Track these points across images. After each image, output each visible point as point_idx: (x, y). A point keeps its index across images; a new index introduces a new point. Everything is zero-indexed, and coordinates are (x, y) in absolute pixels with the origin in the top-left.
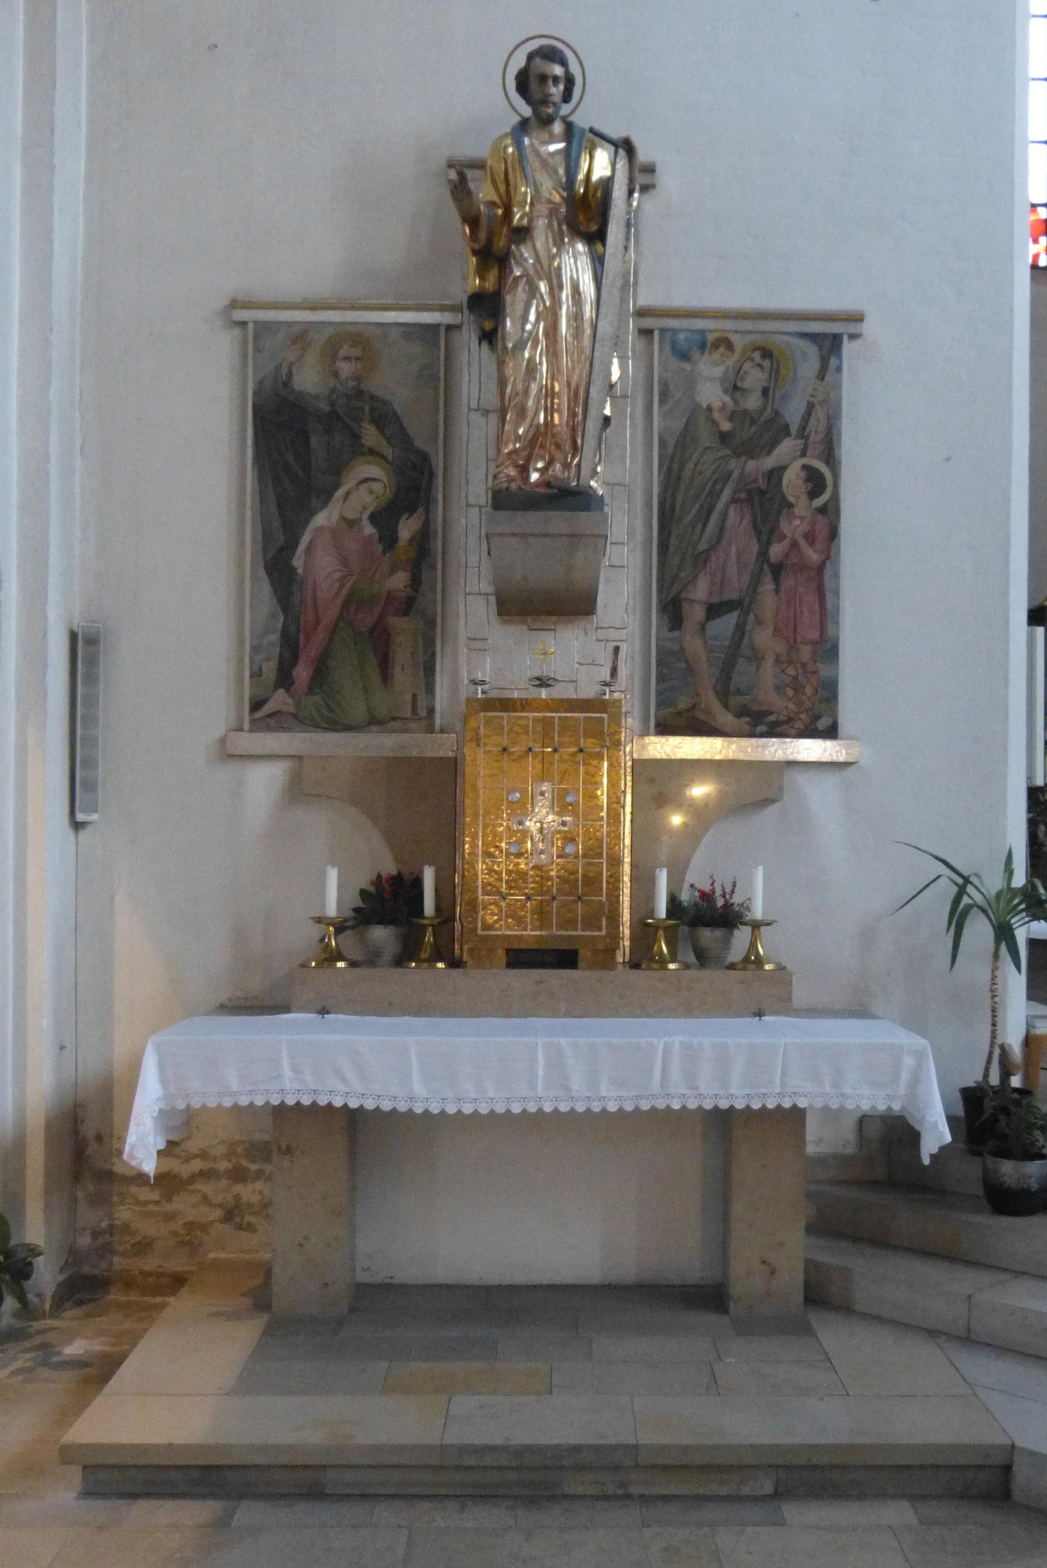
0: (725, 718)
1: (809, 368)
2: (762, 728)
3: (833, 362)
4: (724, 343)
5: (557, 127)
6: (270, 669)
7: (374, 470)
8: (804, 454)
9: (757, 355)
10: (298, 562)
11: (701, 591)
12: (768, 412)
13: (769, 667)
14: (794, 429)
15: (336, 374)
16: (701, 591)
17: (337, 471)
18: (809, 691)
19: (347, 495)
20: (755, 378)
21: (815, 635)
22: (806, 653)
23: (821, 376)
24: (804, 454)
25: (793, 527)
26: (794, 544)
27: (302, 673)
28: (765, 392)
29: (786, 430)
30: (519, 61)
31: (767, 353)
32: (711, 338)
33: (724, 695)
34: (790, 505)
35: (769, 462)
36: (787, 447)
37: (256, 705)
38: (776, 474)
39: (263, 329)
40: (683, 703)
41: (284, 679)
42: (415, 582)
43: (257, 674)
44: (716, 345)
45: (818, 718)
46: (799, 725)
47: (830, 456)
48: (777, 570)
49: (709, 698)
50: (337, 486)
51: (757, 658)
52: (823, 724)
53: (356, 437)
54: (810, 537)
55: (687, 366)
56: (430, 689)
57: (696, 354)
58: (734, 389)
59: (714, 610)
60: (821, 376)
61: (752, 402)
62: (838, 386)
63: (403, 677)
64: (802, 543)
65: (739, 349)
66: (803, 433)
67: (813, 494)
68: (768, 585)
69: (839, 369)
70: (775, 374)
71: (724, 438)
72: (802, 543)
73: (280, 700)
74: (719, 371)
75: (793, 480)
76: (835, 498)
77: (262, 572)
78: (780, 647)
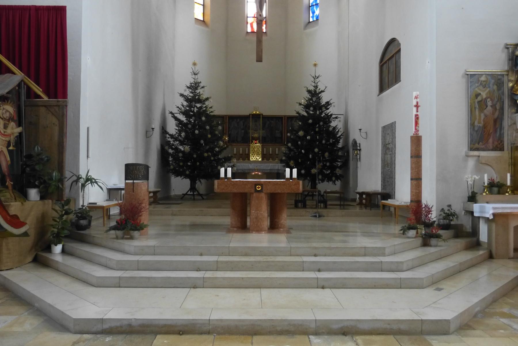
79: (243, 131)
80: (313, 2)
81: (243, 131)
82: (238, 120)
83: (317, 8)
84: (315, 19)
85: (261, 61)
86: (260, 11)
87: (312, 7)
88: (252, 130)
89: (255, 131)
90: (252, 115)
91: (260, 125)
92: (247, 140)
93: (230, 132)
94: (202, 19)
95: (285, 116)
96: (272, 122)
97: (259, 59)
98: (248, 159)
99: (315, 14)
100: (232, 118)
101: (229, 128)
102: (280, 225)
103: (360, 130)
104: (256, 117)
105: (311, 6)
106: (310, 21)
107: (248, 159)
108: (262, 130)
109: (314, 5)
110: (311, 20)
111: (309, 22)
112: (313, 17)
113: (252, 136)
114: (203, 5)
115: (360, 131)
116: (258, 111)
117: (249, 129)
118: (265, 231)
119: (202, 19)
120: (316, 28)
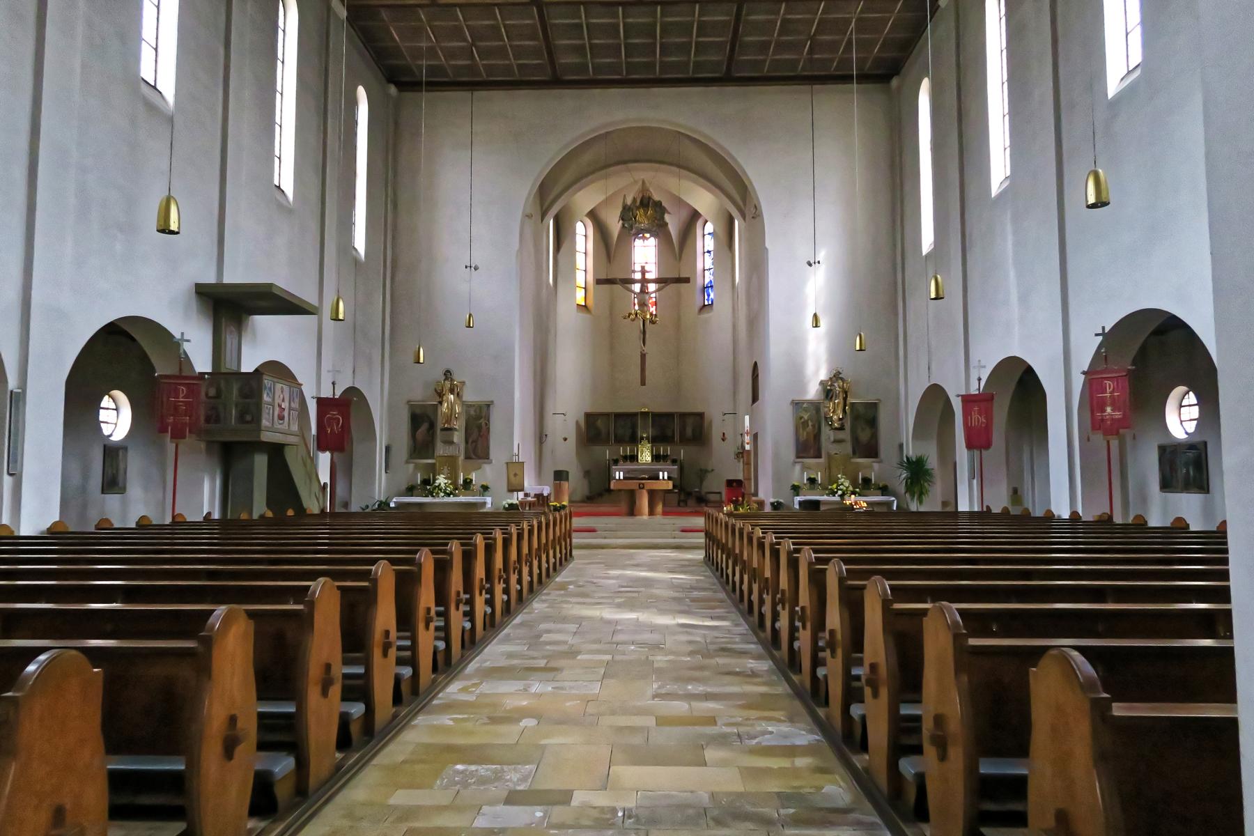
0: (474, 457)
1: (485, 409)
4: (474, 406)
16: (470, 441)
20: (478, 411)
35: (480, 422)
38: (481, 423)
41: (415, 451)
49: (472, 454)
76: (489, 428)
84: (710, 303)
92: (634, 440)
94: (584, 304)
95: (676, 413)
100: (618, 416)
104: (645, 414)
105: (707, 287)
110: (706, 303)
111: (704, 305)
112: (708, 300)
114: (585, 288)
119: (584, 304)
120: (711, 314)
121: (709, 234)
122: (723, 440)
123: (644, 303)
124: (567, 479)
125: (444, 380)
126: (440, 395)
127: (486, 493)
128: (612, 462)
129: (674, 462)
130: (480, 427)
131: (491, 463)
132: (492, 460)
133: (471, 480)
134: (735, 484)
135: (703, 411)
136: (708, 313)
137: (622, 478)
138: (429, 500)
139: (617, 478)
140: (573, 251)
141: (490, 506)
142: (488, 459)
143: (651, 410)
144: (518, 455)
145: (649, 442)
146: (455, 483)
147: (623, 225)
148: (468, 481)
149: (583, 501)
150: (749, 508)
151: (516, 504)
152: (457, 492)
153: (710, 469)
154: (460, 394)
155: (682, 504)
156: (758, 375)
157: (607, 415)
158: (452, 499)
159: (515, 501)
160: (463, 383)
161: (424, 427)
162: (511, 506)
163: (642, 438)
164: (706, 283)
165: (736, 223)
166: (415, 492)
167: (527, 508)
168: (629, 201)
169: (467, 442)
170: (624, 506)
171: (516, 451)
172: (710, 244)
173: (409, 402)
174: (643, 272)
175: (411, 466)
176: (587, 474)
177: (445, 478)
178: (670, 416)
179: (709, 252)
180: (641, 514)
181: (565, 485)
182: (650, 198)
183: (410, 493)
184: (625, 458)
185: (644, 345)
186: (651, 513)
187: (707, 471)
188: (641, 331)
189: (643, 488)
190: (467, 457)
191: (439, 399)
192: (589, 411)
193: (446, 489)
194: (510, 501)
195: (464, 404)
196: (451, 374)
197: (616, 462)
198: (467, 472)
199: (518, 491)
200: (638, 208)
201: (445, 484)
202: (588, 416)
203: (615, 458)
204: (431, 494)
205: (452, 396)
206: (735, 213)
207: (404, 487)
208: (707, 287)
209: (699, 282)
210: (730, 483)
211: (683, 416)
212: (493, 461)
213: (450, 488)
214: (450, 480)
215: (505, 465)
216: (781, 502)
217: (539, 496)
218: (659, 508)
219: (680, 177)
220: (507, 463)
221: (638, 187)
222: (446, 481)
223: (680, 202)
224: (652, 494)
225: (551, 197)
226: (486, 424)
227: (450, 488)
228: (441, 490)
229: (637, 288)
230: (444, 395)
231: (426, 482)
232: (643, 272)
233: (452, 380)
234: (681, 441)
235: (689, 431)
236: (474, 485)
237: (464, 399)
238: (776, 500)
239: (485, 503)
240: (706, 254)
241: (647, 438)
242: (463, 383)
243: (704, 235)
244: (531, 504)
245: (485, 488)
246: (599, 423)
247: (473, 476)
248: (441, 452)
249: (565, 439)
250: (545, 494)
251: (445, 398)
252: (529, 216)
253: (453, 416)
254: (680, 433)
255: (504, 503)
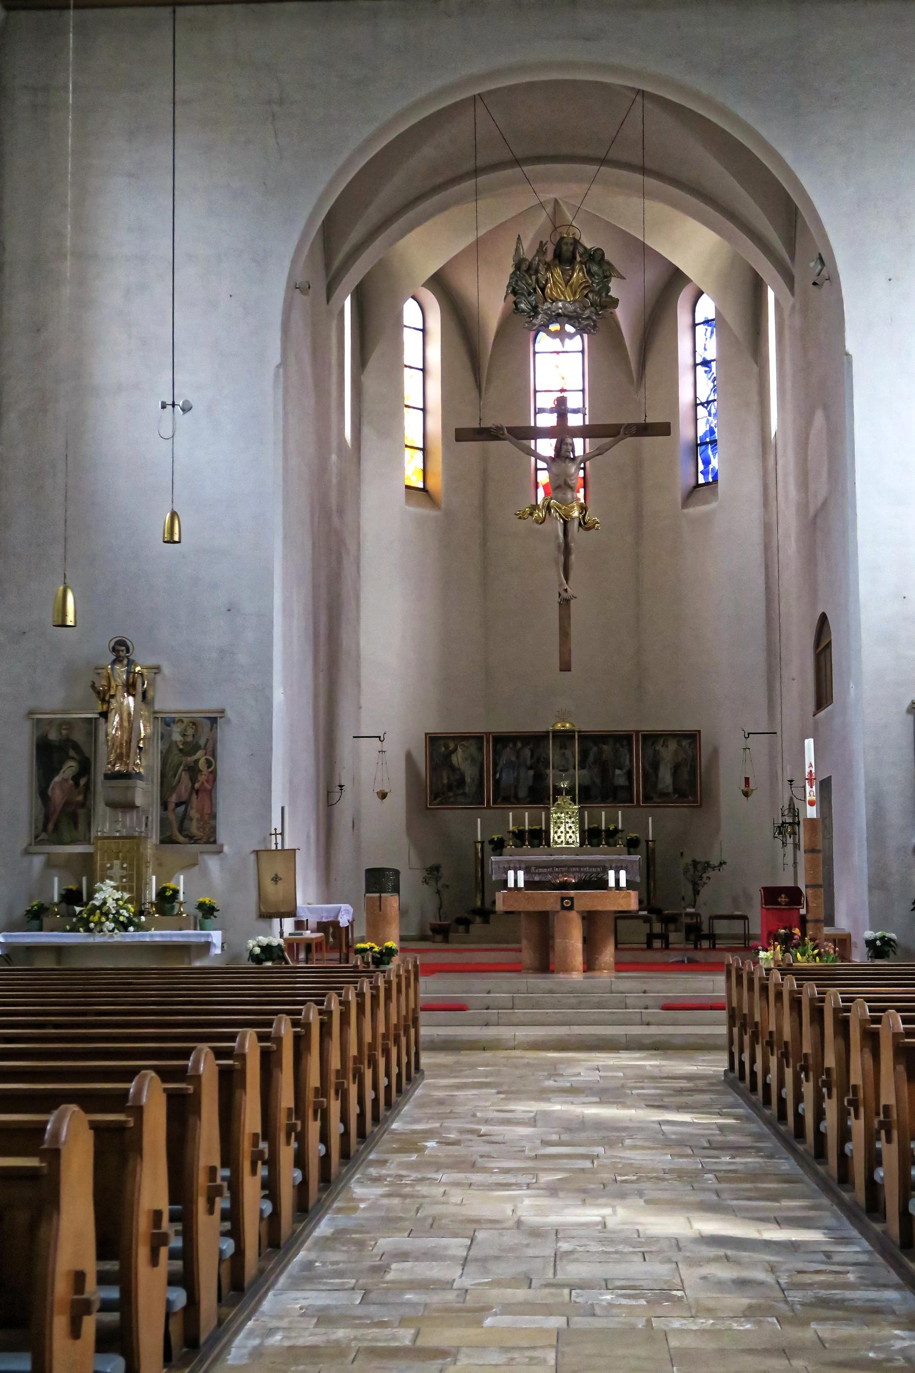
0: (181, 838)
1: (207, 728)
2: (192, 841)
3: (215, 725)
4: (181, 721)
5: (125, 662)
6: (40, 826)
7: (72, 763)
8: (206, 755)
9: (191, 724)
10: (50, 793)
11: (174, 799)
12: (194, 742)
13: (194, 822)
14: (203, 746)
15: (61, 734)
16: (174, 799)
17: (61, 763)
18: (207, 829)
19: (64, 772)
20: (190, 732)
21: (209, 812)
22: (206, 817)
23: (211, 730)
24: (206, 755)
25: (202, 778)
26: (203, 783)
27: (50, 827)
28: (194, 736)
29: (199, 748)
30: (112, 644)
31: (194, 724)
32: (177, 719)
33: (181, 830)
34: (201, 771)
36: (200, 754)
37: (36, 837)
38: (197, 761)
39: (39, 720)
40: (168, 834)
41: (45, 829)
42: (85, 798)
43: (36, 828)
44: (178, 721)
45: (210, 838)
46: (205, 840)
47: (214, 755)
48: (197, 792)
50: (61, 769)
51: (191, 819)
52: (212, 840)
53: (67, 753)
54: (207, 781)
55: (169, 728)
56: (90, 831)
57: (172, 724)
58: (184, 735)
59: (178, 805)
60: (211, 730)
61: (190, 739)
62: (216, 733)
63: (82, 827)
64: (205, 783)
65: (185, 722)
66: (205, 748)
67: (209, 767)
68: (194, 796)
69: (217, 728)
70: (196, 730)
71: (181, 750)
72: (205, 783)
73: (43, 836)
74: (179, 730)
75: (202, 764)
76: (215, 769)
77: (38, 796)
78: (198, 816)
79: (531, 773)
80: (705, 435)
81: (531, 773)
82: (519, 745)
83: (714, 450)
85: (570, 670)
86: (565, 582)
87: (703, 447)
88: (553, 768)
89: (561, 771)
90: (554, 732)
91: (574, 757)
93: (498, 775)
94: (421, 486)
96: (605, 747)
97: (565, 667)
98: (546, 845)
99: (711, 467)
100: (501, 740)
101: (495, 764)
102: (603, 965)
103: (791, 781)
104: (564, 738)
105: (702, 444)
106: (700, 482)
107: (546, 845)
108: (578, 770)
109: (706, 443)
110: (701, 480)
111: (698, 486)
112: (705, 473)
113: (555, 787)
114: (424, 450)
115: (791, 785)
116: (567, 722)
117: (547, 766)
118: (578, 971)
119: (421, 486)
120: (714, 505)
121: (707, 322)
122: (746, 794)
123: (566, 483)
124: (396, 889)
125: (114, 663)
126: (104, 697)
127: (208, 922)
128: (488, 848)
129: (632, 845)
130: (193, 770)
131: (220, 852)
132: (222, 846)
133: (176, 892)
134: (783, 899)
135: (695, 728)
136: (706, 502)
137: (521, 884)
138: (79, 937)
139: (511, 884)
140: (396, 366)
141: (218, 951)
142: (215, 842)
143: (576, 729)
144: (282, 834)
145: (573, 800)
146: (137, 899)
147: (516, 303)
148: (169, 893)
149: (423, 938)
150: (819, 954)
151: (279, 945)
152: (143, 918)
153: (715, 862)
154: (150, 694)
155: (657, 944)
156: (829, 645)
157: (478, 739)
158: (131, 936)
159: (276, 941)
160: (157, 669)
161: (70, 768)
162: (268, 950)
163: (558, 791)
164: (700, 434)
165: (771, 295)
166: (46, 921)
167: (302, 956)
168: (528, 250)
169: (164, 805)
170: (527, 956)
171: (276, 823)
172: (709, 347)
173: (31, 713)
174: (561, 408)
175: (38, 862)
176: (433, 872)
177: (116, 888)
178: (624, 739)
179: (706, 363)
180: (567, 969)
181: (392, 902)
182: (576, 242)
183: (35, 923)
184: (519, 837)
185: (567, 578)
186: (590, 966)
187: (707, 866)
188: (559, 547)
189: (571, 908)
190: (167, 840)
191: (100, 707)
192: (435, 728)
193: (118, 912)
194: (264, 940)
195: (155, 716)
196: (128, 651)
197: (498, 846)
198: (165, 873)
199: (281, 916)
200: (549, 267)
201: (117, 900)
202: (433, 740)
203: (495, 837)
204: (84, 924)
205: (131, 699)
206: (766, 270)
207: (20, 911)
208: (702, 444)
209: (685, 432)
210: (771, 895)
211: (651, 738)
212: (226, 849)
213: (128, 910)
214: (130, 891)
215: (252, 857)
216: (890, 939)
217: (328, 927)
218: (608, 955)
219: (644, 194)
220: (257, 852)
221: (543, 218)
222: (118, 895)
223: (644, 251)
224: (590, 918)
225: (346, 248)
226: (209, 763)
227: (128, 910)
228: (106, 914)
229: (546, 447)
230: (112, 696)
231: (72, 897)
232: (561, 408)
233: (131, 663)
234: (647, 798)
235: (666, 777)
236: (181, 904)
237: (157, 707)
238: (879, 934)
239: (208, 945)
240: (700, 369)
241: (570, 791)
242: (157, 669)
243: (694, 325)
244: (308, 946)
245: (208, 910)
246: (458, 759)
247: (180, 883)
248: (107, 828)
249: (383, 796)
250: (344, 921)
251: (114, 704)
252: (304, 289)
253: (134, 744)
254: (646, 775)
255: (251, 943)
